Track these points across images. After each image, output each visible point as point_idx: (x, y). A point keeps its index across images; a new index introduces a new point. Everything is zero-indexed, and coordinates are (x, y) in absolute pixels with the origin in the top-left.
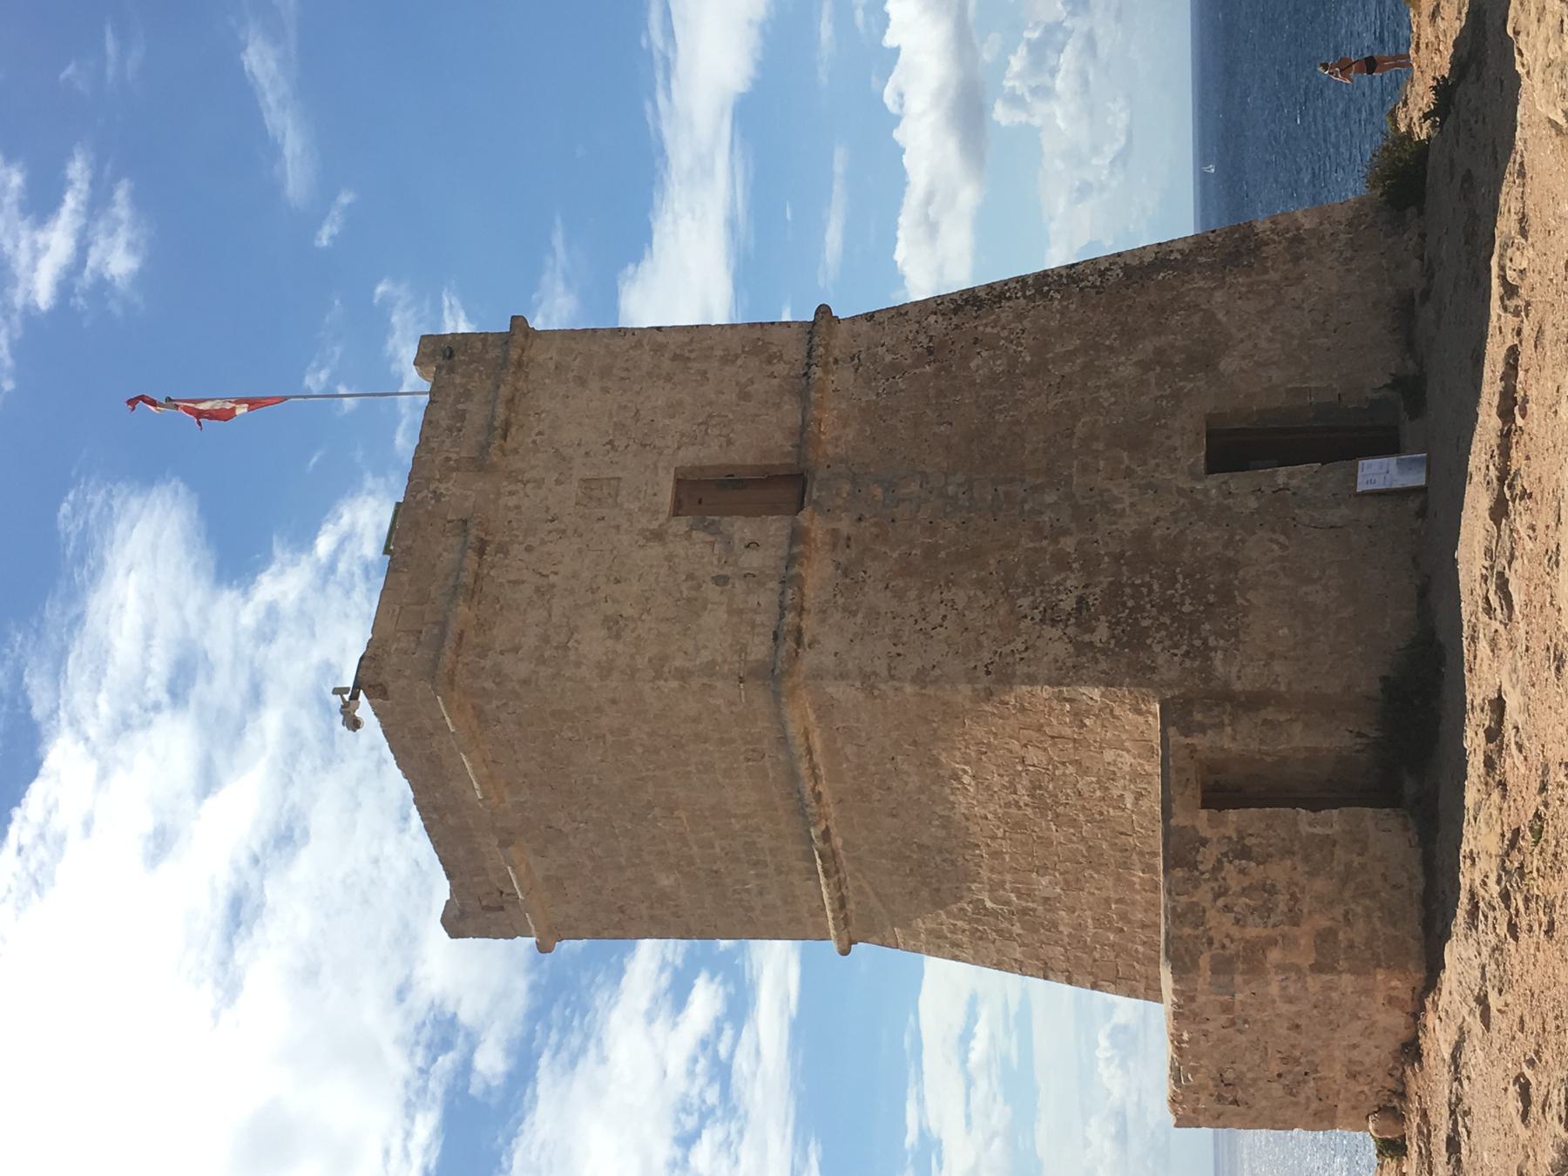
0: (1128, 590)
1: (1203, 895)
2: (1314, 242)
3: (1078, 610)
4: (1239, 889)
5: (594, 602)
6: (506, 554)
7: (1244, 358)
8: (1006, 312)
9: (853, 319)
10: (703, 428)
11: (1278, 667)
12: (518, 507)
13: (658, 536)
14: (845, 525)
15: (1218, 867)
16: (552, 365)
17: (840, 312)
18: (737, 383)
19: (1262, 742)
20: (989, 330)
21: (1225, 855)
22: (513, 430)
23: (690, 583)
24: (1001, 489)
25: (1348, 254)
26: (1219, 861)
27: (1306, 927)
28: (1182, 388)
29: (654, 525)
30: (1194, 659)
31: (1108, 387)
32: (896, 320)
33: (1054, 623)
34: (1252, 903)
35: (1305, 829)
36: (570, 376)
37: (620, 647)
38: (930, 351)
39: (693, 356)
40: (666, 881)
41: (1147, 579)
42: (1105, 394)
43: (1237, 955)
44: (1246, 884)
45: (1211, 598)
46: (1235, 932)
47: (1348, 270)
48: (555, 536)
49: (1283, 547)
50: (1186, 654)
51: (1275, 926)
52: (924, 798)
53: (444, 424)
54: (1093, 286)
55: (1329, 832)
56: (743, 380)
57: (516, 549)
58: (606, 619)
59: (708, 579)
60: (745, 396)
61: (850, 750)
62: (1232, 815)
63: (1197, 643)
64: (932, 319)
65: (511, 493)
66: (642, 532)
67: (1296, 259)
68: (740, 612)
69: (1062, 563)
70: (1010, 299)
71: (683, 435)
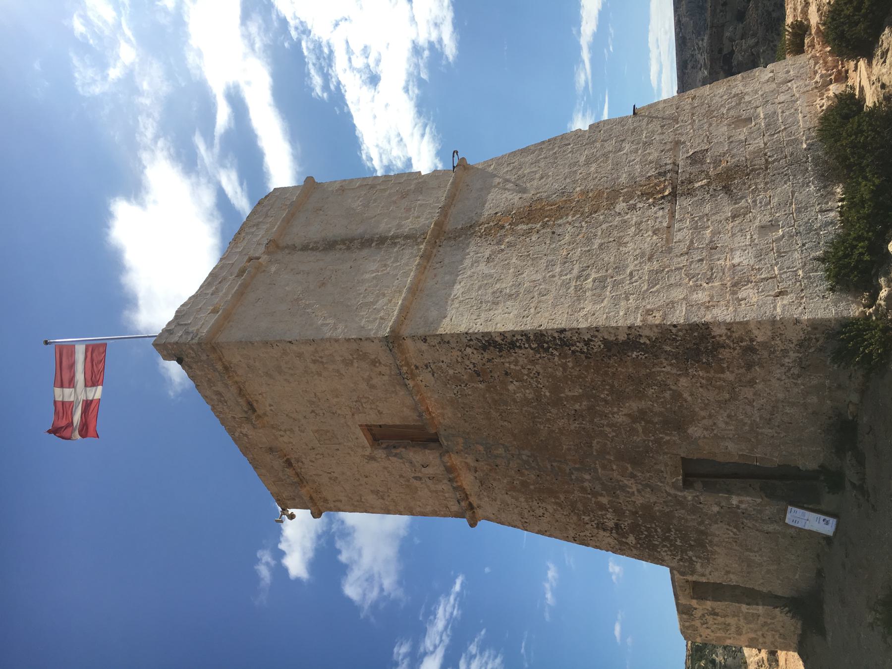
1: (697, 623)
2: (765, 354)
7: (706, 429)
8: (522, 356)
11: (732, 576)
22: (255, 404)
24: (555, 464)
25: (796, 371)
28: (662, 438)
31: (608, 425)
41: (654, 526)
42: (607, 429)
45: (692, 543)
46: (712, 634)
47: (796, 384)
49: (735, 534)
50: (681, 560)
54: (582, 352)
67: (749, 366)
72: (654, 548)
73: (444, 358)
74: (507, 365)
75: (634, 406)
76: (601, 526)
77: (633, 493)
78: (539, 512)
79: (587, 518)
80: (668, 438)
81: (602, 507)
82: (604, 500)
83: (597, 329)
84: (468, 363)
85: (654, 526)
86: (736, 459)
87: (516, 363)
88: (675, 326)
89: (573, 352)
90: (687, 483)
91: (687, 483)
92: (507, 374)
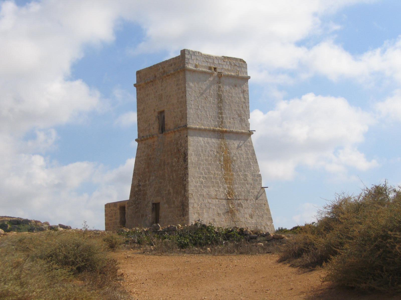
13: (155, 111)
45: (137, 206)
72: (135, 196)
73: (182, 141)
74: (181, 159)
75: (171, 191)
76: (139, 181)
77: (150, 190)
78: (142, 162)
81: (146, 181)
82: (147, 182)
83: (188, 183)
84: (181, 148)
85: (141, 195)
86: (160, 215)
87: (181, 161)
88: (188, 200)
89: (183, 177)
90: (153, 204)
91: (153, 204)
92: (179, 158)
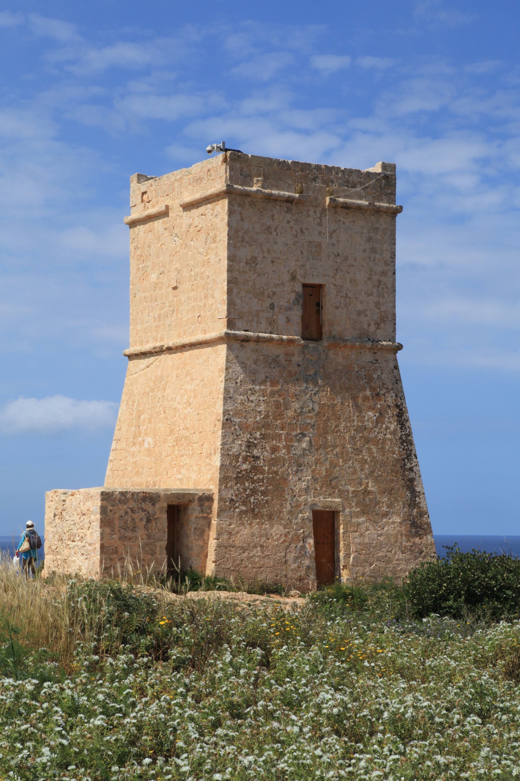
0: (261, 477)
3: (253, 457)
4: (134, 517)
5: (263, 252)
6: (287, 212)
9: (396, 360)
10: (345, 296)
12: (308, 215)
13: (293, 278)
14: (297, 359)
15: (143, 510)
16: (377, 226)
17: (400, 355)
18: (366, 310)
19: (195, 529)
20: (387, 420)
21: (148, 513)
22: (346, 211)
23: (271, 293)
26: (145, 511)
27: (119, 543)
28: (353, 501)
29: (298, 276)
30: (230, 503)
32: (394, 379)
33: (248, 447)
34: (128, 522)
35: (158, 544)
36: (372, 234)
37: (242, 264)
38: (378, 394)
39: (380, 289)
40: (154, 277)
43: (107, 516)
44: (137, 521)
45: (257, 510)
46: (117, 515)
48: (294, 233)
50: (232, 500)
51: (119, 531)
52: (182, 391)
53: (351, 179)
54: (405, 465)
55: (157, 553)
56: (367, 313)
57: (289, 216)
58: (255, 258)
59: (273, 301)
60: (359, 313)
61: (201, 361)
62: (165, 516)
63: (237, 505)
64: (394, 395)
65: (315, 212)
66: (295, 271)
68: (257, 315)
69: (275, 449)
70: (401, 428)
71: (341, 287)
79: (258, 435)
80: (353, 504)
87: (391, 423)
89: (404, 460)
